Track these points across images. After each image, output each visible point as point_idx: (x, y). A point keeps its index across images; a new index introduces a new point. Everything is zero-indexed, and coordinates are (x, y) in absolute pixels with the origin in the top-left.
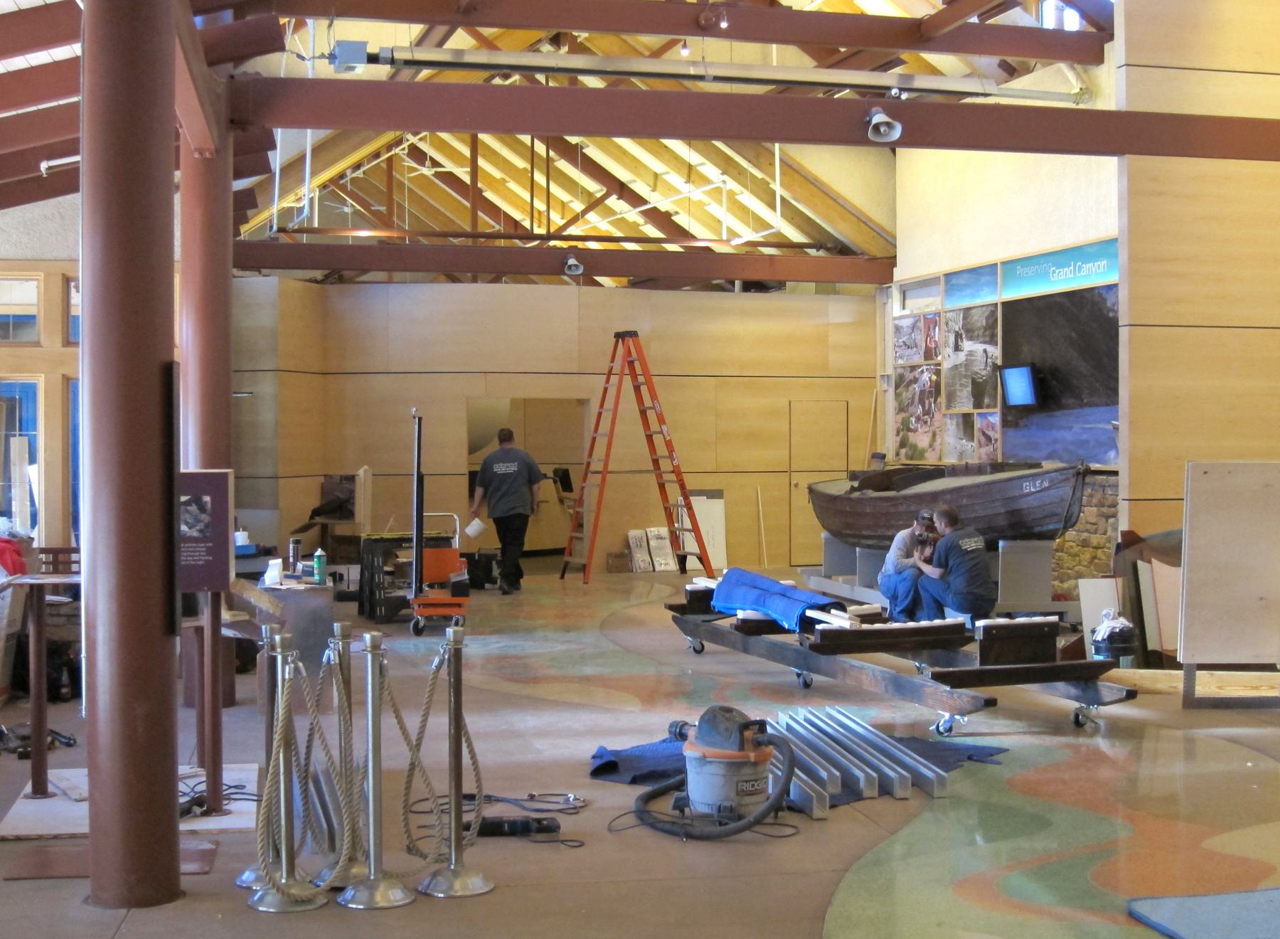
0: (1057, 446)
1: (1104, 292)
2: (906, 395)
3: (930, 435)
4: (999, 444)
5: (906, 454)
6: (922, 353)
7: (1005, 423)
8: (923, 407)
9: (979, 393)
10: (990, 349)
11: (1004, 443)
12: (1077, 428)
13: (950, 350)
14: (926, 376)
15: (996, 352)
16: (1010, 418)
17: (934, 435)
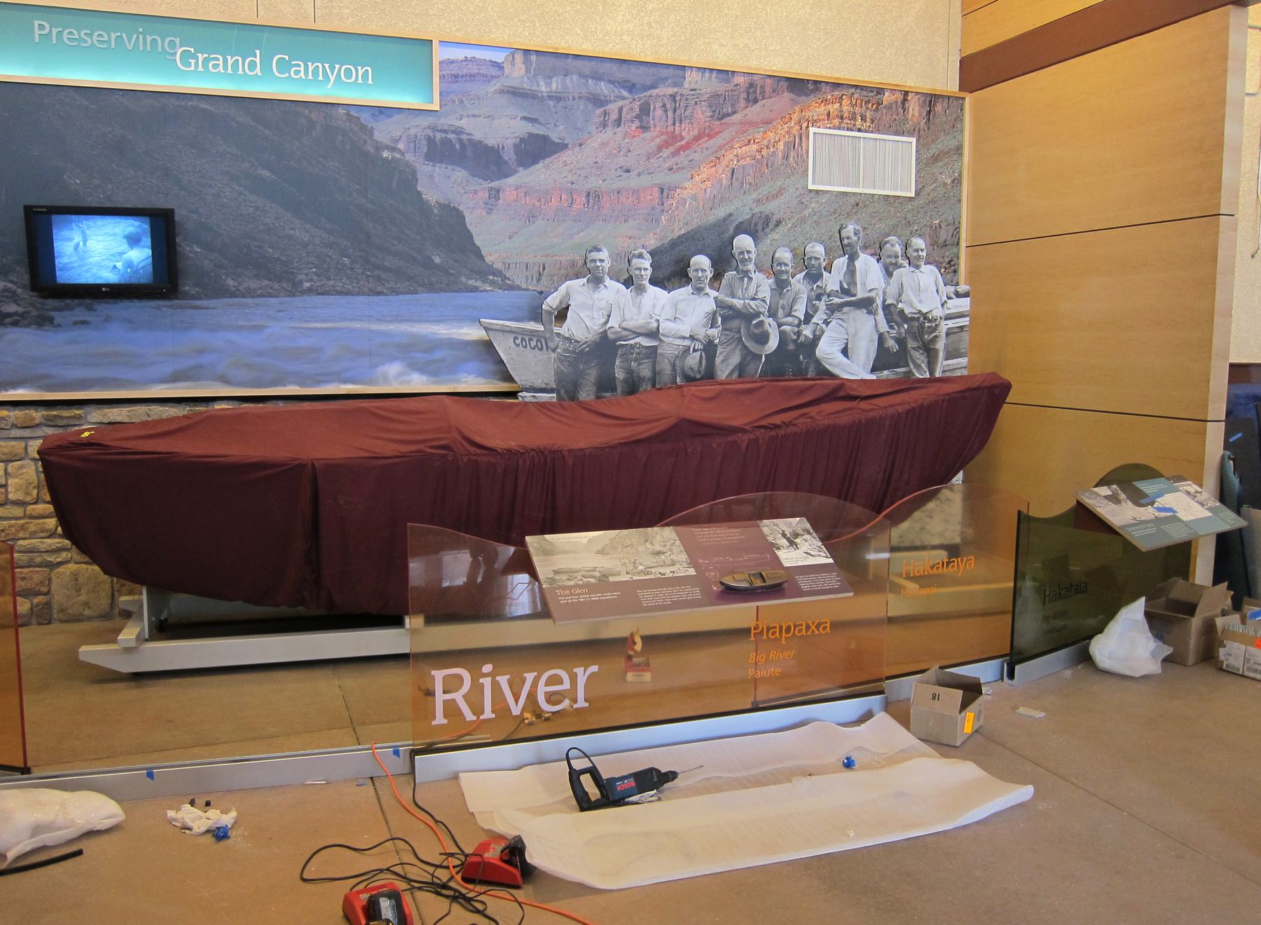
1: (365, 117)
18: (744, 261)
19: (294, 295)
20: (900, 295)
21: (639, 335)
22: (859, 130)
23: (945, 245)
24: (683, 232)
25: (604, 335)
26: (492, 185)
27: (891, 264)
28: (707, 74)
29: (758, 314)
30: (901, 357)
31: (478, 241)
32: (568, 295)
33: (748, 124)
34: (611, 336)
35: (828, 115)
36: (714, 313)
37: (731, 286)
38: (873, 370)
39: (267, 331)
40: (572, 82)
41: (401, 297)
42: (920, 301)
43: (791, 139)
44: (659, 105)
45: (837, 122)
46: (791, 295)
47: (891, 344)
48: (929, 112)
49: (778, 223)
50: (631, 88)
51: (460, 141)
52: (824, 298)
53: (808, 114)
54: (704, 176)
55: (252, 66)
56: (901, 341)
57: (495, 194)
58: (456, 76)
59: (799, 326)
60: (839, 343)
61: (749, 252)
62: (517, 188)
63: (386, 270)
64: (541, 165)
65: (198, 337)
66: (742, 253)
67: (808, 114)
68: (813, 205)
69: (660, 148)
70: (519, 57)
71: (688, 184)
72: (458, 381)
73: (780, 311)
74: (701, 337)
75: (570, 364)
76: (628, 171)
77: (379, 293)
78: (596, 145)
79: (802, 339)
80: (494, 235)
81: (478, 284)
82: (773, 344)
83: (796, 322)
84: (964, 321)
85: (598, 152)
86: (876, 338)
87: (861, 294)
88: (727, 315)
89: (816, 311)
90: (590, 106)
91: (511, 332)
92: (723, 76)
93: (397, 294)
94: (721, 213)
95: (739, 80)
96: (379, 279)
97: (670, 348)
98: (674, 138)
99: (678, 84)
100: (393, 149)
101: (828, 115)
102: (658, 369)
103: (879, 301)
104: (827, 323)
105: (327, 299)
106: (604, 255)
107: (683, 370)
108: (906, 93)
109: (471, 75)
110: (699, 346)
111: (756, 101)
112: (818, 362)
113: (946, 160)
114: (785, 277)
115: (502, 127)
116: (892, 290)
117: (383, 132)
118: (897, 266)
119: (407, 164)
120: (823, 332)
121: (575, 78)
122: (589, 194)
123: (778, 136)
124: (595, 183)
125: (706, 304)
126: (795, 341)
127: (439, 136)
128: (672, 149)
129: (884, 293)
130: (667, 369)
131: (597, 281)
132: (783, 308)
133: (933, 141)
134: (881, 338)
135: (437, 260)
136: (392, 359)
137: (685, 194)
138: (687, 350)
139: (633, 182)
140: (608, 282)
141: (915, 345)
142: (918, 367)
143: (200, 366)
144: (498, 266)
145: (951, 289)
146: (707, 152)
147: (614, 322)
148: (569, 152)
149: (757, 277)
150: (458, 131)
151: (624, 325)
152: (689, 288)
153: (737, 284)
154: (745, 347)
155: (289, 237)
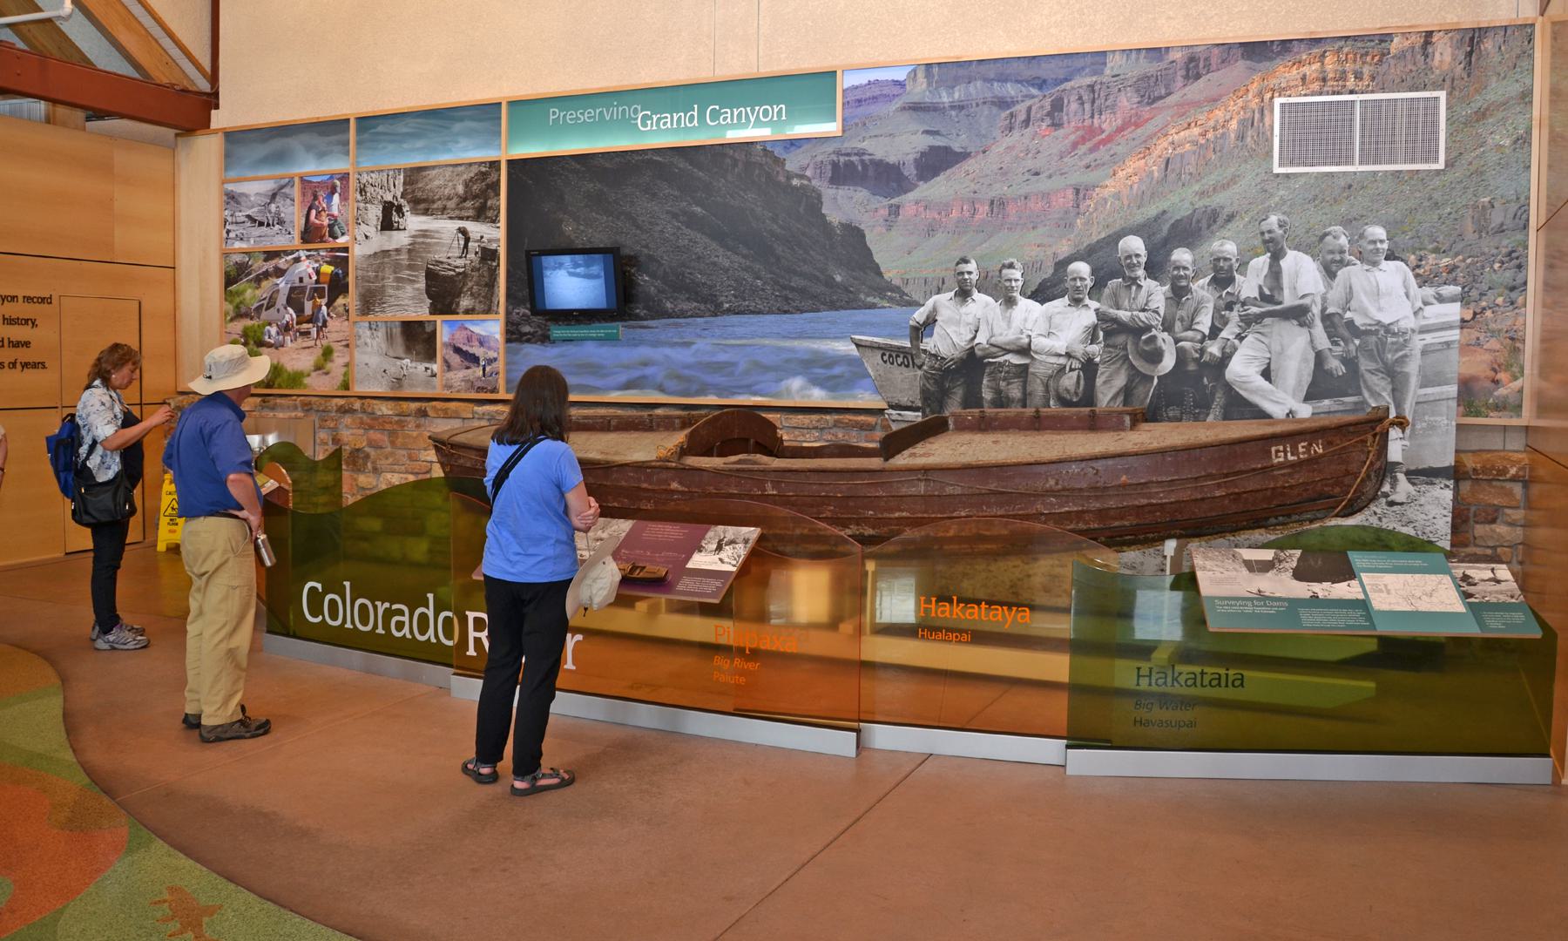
0: (649, 371)
1: (778, 152)
2: (251, 295)
3: (318, 352)
4: (500, 365)
6: (296, 234)
7: (514, 334)
8: (299, 310)
9: (443, 292)
10: (475, 228)
11: (507, 364)
12: (701, 344)
13: (371, 231)
14: (306, 267)
15: (495, 234)
16: (526, 329)
17: (328, 353)
18: (1132, 267)
20: (1348, 302)
21: (1009, 351)
22: (1352, 92)
23: (1501, 230)
24: (1103, 235)
26: (895, 201)
27: (1334, 261)
28: (1134, 55)
29: (1148, 328)
30: (1352, 380)
31: (877, 259)
33: (1184, 108)
35: (1304, 78)
36: (1095, 328)
38: (1308, 398)
39: (694, 347)
40: (977, 89)
41: (805, 315)
42: (1380, 309)
43: (1249, 115)
44: (1074, 98)
45: (1316, 86)
47: (1335, 365)
48: (1470, 54)
49: (1231, 218)
50: (1041, 84)
51: (862, 162)
52: (1237, 307)
55: (692, 119)
56: (1350, 362)
57: (895, 210)
58: (859, 101)
59: (1202, 341)
60: (1257, 363)
61: (1137, 256)
62: (917, 203)
63: (793, 289)
64: (941, 178)
65: (644, 352)
66: (1129, 257)
67: (1273, 82)
68: (1281, 193)
69: (1075, 145)
70: (921, 74)
72: (855, 397)
73: (1178, 326)
74: (1079, 355)
76: (1037, 174)
77: (786, 312)
78: (1001, 149)
79: (1206, 358)
80: (892, 254)
81: (876, 300)
82: (1168, 363)
83: (1199, 337)
84: (1454, 335)
86: (1312, 356)
87: (1288, 300)
88: (1108, 328)
89: (1226, 324)
90: (995, 110)
91: (879, 348)
94: (1152, 211)
95: (1176, 55)
96: (786, 299)
97: (1042, 367)
98: (1091, 132)
99: (1101, 73)
100: (802, 177)
101: (1304, 78)
102: (1029, 389)
103: (1316, 310)
104: (1240, 338)
106: (972, 266)
108: (1429, 34)
110: (1076, 364)
111: (1198, 77)
112: (1229, 388)
113: (1500, 115)
114: (1184, 283)
115: (901, 144)
116: (1337, 293)
117: (793, 163)
118: (1343, 263)
119: (814, 190)
120: (1236, 349)
121: (979, 83)
122: (992, 203)
123: (1229, 115)
125: (1086, 317)
126: (1197, 360)
127: (842, 159)
128: (1089, 145)
129: (1324, 299)
130: (1038, 389)
131: (964, 294)
132: (1182, 319)
133: (1477, 91)
134: (1319, 358)
135: (838, 278)
136: (795, 374)
137: (1106, 193)
138: (1062, 370)
139: (1043, 184)
140: (976, 295)
141: (1372, 366)
143: (644, 377)
144: (897, 282)
145: (1429, 291)
146: (1133, 143)
147: (982, 339)
148: (971, 161)
149: (1148, 284)
151: (993, 340)
153: (1123, 293)
154: (1132, 367)
155: (715, 264)
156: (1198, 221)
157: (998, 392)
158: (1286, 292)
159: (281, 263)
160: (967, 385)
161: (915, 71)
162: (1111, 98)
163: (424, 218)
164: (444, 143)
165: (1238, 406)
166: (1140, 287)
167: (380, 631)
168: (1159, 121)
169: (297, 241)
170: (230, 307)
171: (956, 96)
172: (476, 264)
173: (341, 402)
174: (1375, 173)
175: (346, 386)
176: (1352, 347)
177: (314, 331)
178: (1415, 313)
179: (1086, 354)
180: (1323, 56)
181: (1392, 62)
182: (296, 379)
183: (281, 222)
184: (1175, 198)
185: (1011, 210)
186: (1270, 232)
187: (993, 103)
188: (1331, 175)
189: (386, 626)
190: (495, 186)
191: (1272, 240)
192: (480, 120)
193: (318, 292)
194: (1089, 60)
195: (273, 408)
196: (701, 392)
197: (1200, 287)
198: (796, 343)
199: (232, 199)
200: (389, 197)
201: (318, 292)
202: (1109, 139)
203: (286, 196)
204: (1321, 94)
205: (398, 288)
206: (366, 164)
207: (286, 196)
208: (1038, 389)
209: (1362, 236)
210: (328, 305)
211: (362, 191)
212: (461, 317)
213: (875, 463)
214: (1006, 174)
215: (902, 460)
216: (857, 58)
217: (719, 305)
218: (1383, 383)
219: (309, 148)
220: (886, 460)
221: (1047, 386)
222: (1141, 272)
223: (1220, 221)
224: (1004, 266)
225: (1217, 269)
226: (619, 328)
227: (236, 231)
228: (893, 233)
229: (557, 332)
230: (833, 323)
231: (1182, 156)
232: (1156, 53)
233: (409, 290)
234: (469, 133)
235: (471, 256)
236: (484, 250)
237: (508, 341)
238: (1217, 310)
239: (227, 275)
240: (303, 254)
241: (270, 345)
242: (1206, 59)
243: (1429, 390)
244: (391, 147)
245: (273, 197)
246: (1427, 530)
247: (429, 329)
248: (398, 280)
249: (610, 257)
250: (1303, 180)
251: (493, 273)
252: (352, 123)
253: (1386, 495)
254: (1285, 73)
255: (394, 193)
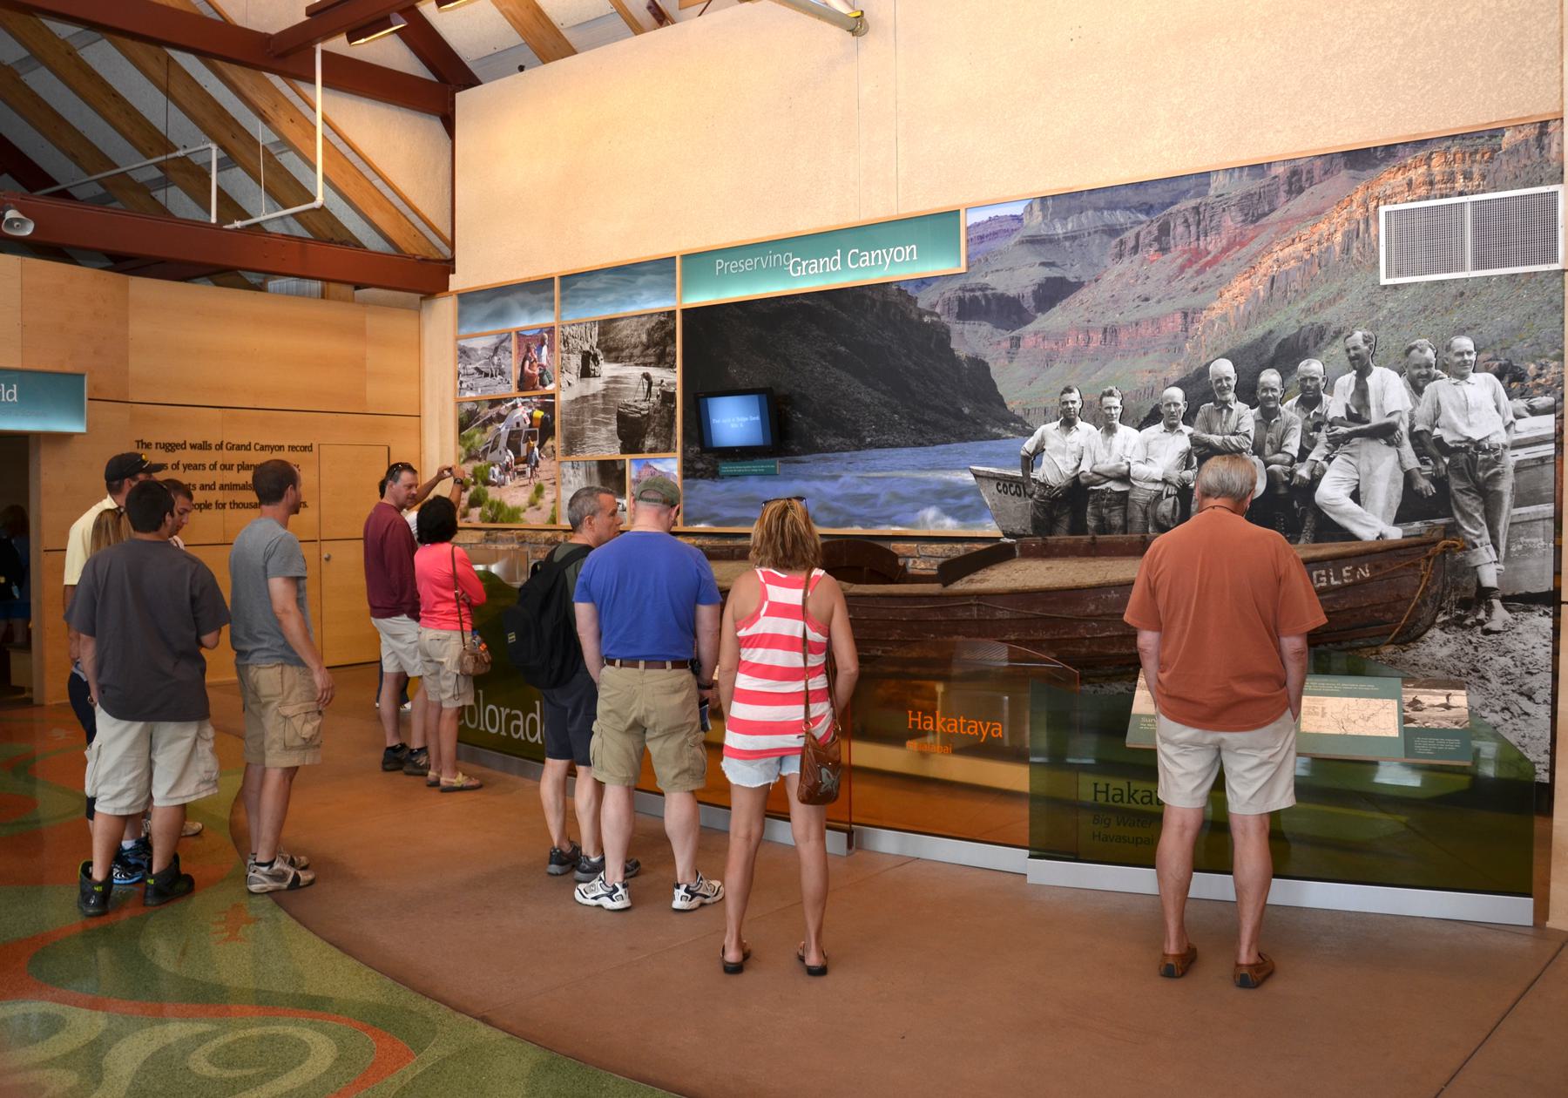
1: (910, 290)
2: (480, 439)
3: (532, 489)
5: (483, 517)
6: (514, 383)
8: (517, 452)
9: (632, 433)
10: (657, 373)
12: (848, 478)
13: (573, 378)
14: (522, 413)
15: (671, 378)
16: (700, 466)
18: (1222, 390)
19: (859, 449)
20: (1436, 417)
21: (1110, 479)
22: (1461, 194)
25: (1076, 479)
27: (1420, 376)
28: (1236, 174)
31: (1001, 390)
32: (1043, 440)
34: (1083, 481)
36: (1189, 453)
37: (1207, 420)
38: (1398, 521)
39: (841, 480)
40: (1088, 219)
42: (1469, 425)
43: (1354, 226)
44: (1180, 221)
45: (1423, 191)
46: (1280, 427)
47: (1423, 484)
49: (1338, 334)
50: (1148, 209)
51: (985, 296)
52: (1325, 428)
53: (1377, 190)
54: (1236, 291)
56: (1439, 481)
57: (1016, 342)
58: (982, 237)
59: (1291, 464)
60: (1346, 485)
61: (1228, 379)
64: (1058, 307)
65: (797, 486)
66: (1220, 380)
67: (1377, 190)
69: (1182, 269)
70: (1036, 207)
71: (1215, 304)
72: (983, 526)
73: (1268, 448)
74: (1174, 481)
75: (1045, 511)
76: (1147, 300)
77: (921, 445)
78: (1112, 277)
81: (1001, 431)
83: (1288, 459)
85: (1119, 284)
86: (1401, 476)
87: (1376, 419)
88: (1201, 452)
90: (1105, 238)
92: (1256, 171)
93: (935, 444)
94: (1258, 331)
95: (1279, 170)
96: (921, 432)
97: (1143, 492)
98: (1197, 254)
99: (1205, 194)
100: (932, 314)
101: (1410, 184)
102: (1129, 516)
103: (1404, 428)
104: (1329, 459)
105: (884, 452)
106: (1075, 396)
107: (1155, 517)
109: (995, 233)
111: (1301, 190)
112: (1318, 511)
114: (1272, 405)
115: (1018, 277)
116: (1424, 409)
118: (1430, 378)
119: (943, 326)
120: (1324, 471)
121: (1090, 213)
122: (1105, 330)
123: (1333, 228)
124: (1113, 317)
125: (1180, 442)
126: (1287, 484)
127: (967, 295)
128: (1196, 267)
129: (1412, 416)
130: (1138, 516)
131: (1068, 424)
132: (1271, 442)
134: (1409, 478)
135: (966, 411)
136: (929, 504)
137: (1213, 315)
138: (1159, 496)
139: (1153, 310)
140: (1080, 424)
141: (1463, 485)
142: (1468, 517)
144: (1019, 412)
145: (1521, 404)
146: (1238, 264)
148: (1085, 290)
149: (1239, 407)
150: (984, 288)
152: (1161, 426)
153: (1215, 416)
155: (857, 400)
156: (1305, 340)
157: (1101, 519)
158: (1373, 410)
159: (503, 409)
160: (1078, 513)
161: (1031, 205)
162: (1216, 218)
163: (614, 366)
164: (630, 296)
165: (1328, 529)
166: (1230, 410)
167: (503, 733)
168: (1264, 237)
169: (514, 390)
170: (463, 450)
171: (1070, 227)
172: (658, 406)
173: (548, 534)
174: (1488, 278)
175: (553, 520)
176: (1441, 466)
177: (528, 470)
178: (1507, 428)
179: (1181, 479)
180: (1430, 158)
181: (1504, 158)
182: (514, 514)
183: (502, 373)
184: (1281, 317)
185: (1123, 336)
186: (1355, 348)
187: (1104, 232)
188: (1442, 282)
189: (508, 730)
190: (672, 333)
191: (1357, 357)
192: (660, 273)
193: (532, 435)
194: (1193, 181)
195: (495, 541)
196: (847, 523)
197: (1289, 410)
198: (929, 475)
199: (464, 353)
200: (587, 348)
201: (532, 435)
202: (1215, 260)
203: (506, 349)
204: (1428, 198)
205: (595, 430)
206: (569, 317)
207: (506, 349)
208: (1138, 516)
209: (1448, 348)
210: (540, 447)
211: (565, 342)
212: (646, 456)
213: (935, 588)
214: (1116, 302)
215: (960, 586)
216: (985, 195)
217: (862, 440)
218: (1475, 504)
219: (523, 305)
220: (945, 585)
221: (1145, 513)
222: (1231, 396)
223: (1327, 338)
224: (1104, 394)
225: (1304, 389)
226: (776, 464)
227: (467, 381)
228: (1015, 364)
229: (726, 468)
230: (963, 453)
231: (1287, 273)
232: (1258, 169)
233: (604, 432)
234: (650, 286)
235: (654, 399)
236: (664, 393)
237: (685, 477)
238: (1305, 431)
239: (461, 421)
240: (519, 401)
241: (494, 484)
242: (1309, 172)
243: (1524, 510)
244: (588, 301)
245: (496, 349)
246: (1526, 661)
247: (620, 467)
248: (595, 422)
249: (764, 397)
250: (1411, 291)
251: (672, 413)
252: (557, 282)
253: (1481, 623)
254: (1390, 179)
255: (591, 343)
